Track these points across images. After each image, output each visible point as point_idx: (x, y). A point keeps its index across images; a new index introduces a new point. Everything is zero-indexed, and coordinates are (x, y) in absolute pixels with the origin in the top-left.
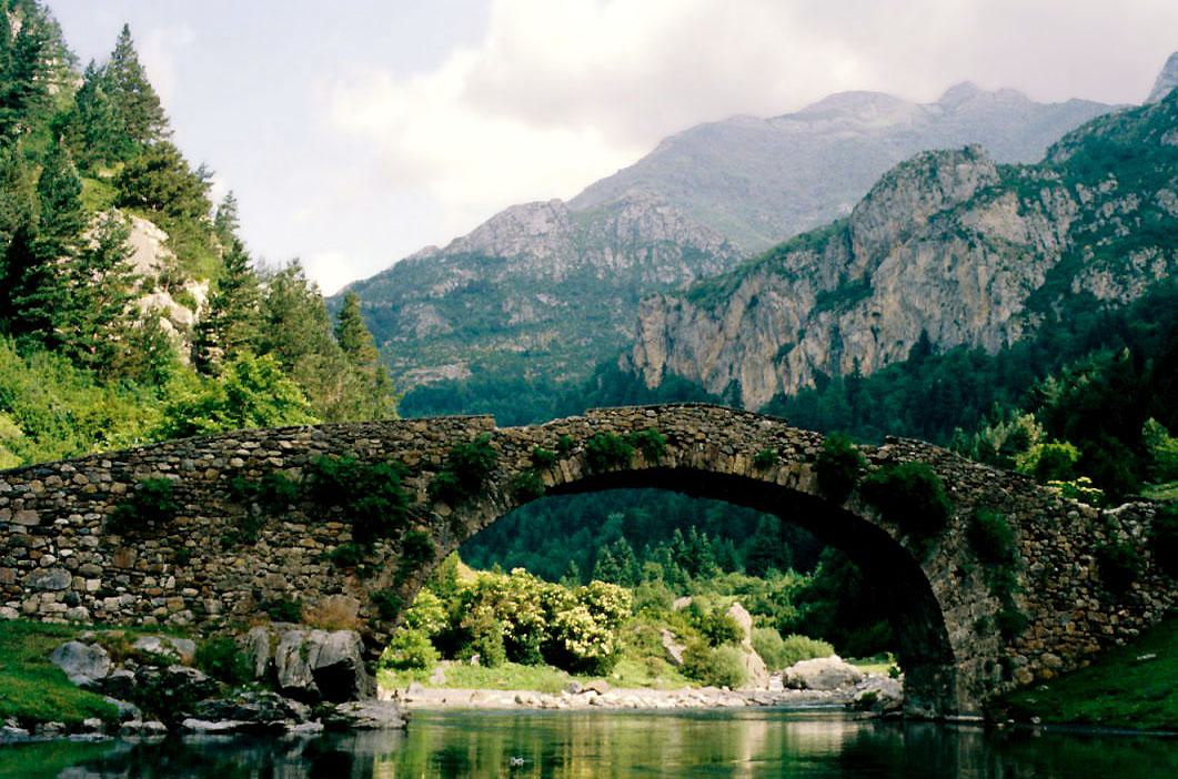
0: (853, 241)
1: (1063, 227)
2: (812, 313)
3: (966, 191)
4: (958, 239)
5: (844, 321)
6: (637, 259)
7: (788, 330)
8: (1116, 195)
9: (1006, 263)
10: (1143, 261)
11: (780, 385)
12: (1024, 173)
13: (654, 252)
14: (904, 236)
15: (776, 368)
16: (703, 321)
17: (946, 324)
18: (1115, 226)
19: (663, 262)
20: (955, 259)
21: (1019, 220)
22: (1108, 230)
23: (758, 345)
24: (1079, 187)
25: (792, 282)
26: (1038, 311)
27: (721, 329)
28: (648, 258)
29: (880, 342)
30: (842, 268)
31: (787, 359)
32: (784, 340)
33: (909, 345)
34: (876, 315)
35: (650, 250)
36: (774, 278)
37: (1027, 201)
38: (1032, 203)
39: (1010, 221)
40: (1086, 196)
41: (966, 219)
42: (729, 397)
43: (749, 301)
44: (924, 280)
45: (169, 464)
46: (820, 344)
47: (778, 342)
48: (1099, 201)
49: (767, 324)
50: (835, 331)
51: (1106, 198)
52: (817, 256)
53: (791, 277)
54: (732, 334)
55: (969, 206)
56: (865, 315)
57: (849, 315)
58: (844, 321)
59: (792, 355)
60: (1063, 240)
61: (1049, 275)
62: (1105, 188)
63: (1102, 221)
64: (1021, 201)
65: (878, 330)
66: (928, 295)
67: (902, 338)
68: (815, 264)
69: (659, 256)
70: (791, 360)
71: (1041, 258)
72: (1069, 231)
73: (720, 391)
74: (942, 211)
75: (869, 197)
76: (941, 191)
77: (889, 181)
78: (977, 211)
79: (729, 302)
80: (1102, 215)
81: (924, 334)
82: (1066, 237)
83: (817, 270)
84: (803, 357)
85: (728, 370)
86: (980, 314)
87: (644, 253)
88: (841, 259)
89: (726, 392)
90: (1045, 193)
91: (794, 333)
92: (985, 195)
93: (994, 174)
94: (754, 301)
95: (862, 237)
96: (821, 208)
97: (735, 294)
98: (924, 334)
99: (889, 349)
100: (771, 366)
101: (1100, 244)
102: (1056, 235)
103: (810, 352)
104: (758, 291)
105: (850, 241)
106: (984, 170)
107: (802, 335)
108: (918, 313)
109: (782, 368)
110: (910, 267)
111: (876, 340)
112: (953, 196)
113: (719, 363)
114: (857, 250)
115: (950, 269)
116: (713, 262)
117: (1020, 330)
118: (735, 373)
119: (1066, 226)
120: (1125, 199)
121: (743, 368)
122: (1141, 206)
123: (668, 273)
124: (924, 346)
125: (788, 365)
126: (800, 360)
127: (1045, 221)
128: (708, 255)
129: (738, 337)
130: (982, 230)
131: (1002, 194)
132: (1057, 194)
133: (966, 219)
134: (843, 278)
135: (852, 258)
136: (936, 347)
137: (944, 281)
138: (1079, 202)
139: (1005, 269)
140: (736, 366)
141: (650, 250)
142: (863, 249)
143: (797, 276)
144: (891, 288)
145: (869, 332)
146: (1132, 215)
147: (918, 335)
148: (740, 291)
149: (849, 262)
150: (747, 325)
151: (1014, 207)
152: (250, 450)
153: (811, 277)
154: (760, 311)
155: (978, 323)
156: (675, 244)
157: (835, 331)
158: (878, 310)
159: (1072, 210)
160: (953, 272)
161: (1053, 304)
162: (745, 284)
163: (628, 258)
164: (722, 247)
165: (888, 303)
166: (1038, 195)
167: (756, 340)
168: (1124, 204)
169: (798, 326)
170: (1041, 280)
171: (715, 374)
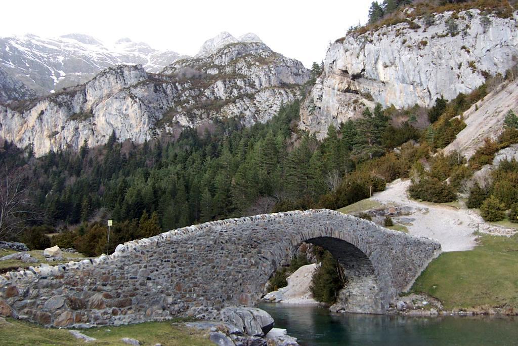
0: (87, 94)
2: (68, 120)
3: (134, 81)
5: (81, 126)
11: (52, 147)
14: (109, 96)
15: (50, 140)
16: (17, 117)
18: (189, 100)
20: (128, 106)
23: (42, 131)
24: (177, 84)
29: (95, 134)
30: (81, 104)
31: (55, 137)
33: (107, 138)
34: (94, 124)
37: (158, 87)
40: (179, 88)
41: (134, 91)
42: (28, 150)
43: (40, 112)
44: (115, 113)
46: (70, 133)
49: (48, 122)
51: (187, 89)
53: (60, 105)
54: (31, 125)
55: (135, 87)
56: (90, 124)
57: (84, 122)
58: (81, 126)
59: (57, 136)
63: (185, 97)
64: (155, 87)
66: (116, 119)
67: (105, 134)
70: (57, 138)
73: (24, 147)
77: (104, 73)
79: (30, 112)
80: (185, 95)
81: (114, 133)
84: (63, 138)
85: (28, 139)
86: (137, 128)
89: (27, 147)
90: (164, 85)
93: (146, 76)
94: (42, 113)
97: (33, 109)
98: (114, 133)
99: (99, 138)
101: (184, 105)
104: (44, 109)
105: (86, 95)
107: (63, 128)
108: (112, 125)
109: (53, 141)
110: (110, 108)
111: (94, 134)
112: (129, 83)
114: (88, 98)
115: (126, 110)
116: (17, 93)
122: (199, 94)
124: (114, 138)
127: (164, 95)
128: (15, 90)
129: (33, 126)
131: (149, 84)
132: (169, 86)
133: (134, 91)
134: (81, 108)
135: (85, 101)
136: (118, 139)
137: (123, 114)
140: (31, 138)
142: (91, 98)
143: (62, 105)
144: (101, 115)
145: (91, 130)
147: (111, 134)
148: (36, 108)
149: (85, 102)
151: (152, 89)
153: (68, 107)
154: (45, 117)
157: (77, 129)
158: (96, 122)
160: (127, 111)
161: (166, 126)
162: (38, 105)
165: (100, 120)
166: (162, 85)
171: (21, 140)
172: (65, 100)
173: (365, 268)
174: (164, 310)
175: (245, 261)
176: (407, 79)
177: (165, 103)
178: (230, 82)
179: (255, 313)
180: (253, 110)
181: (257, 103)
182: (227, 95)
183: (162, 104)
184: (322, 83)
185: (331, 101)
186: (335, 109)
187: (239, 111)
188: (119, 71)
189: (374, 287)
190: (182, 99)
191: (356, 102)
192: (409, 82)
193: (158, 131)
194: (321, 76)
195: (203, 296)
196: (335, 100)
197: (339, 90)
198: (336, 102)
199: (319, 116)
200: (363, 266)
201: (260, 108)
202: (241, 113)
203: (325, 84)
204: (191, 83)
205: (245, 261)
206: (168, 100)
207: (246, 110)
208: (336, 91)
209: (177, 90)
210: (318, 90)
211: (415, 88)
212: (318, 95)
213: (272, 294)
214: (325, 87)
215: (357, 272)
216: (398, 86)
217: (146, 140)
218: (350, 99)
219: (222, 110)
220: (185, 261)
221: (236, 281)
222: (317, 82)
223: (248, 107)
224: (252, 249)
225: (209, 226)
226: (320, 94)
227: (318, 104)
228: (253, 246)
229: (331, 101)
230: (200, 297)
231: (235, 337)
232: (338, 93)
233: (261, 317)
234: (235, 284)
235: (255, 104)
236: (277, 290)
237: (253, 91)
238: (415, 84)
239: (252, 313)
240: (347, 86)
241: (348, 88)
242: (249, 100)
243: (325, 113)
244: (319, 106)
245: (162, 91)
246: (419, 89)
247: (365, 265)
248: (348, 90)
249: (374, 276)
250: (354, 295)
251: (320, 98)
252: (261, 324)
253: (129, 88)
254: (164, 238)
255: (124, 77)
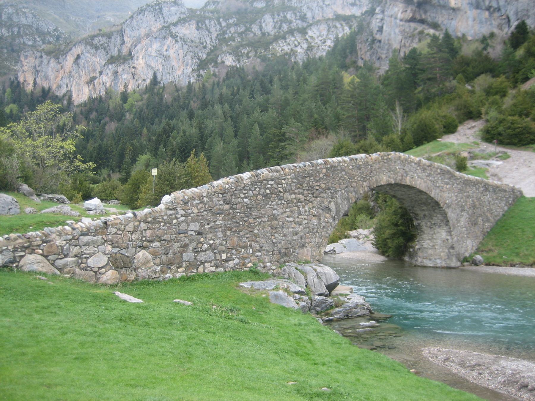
0: (124, 35)
1: (214, 35)
2: (105, 64)
3: (174, 19)
4: (170, 38)
6: (13, 32)
7: (94, 70)
8: (236, 25)
9: (191, 49)
10: (246, 52)
12: (198, 13)
13: (22, 29)
14: (147, 36)
15: (89, 87)
17: (164, 73)
18: (234, 38)
19: (27, 35)
20: (168, 46)
21: (196, 32)
22: (232, 39)
23: (80, 77)
24: (221, 20)
25: (96, 50)
26: (203, 69)
27: (62, 68)
28: (19, 32)
30: (119, 46)
32: (92, 75)
33: (148, 82)
34: (134, 67)
35: (19, 28)
36: (88, 47)
37: (200, 24)
38: (202, 25)
39: (193, 32)
40: (224, 24)
41: (174, 29)
42: (67, 98)
43: (76, 57)
44: (155, 55)
45: (244, 194)
46: (109, 77)
47: (90, 75)
48: (229, 26)
49: (85, 67)
50: (116, 73)
52: (108, 40)
53: (96, 48)
54: (67, 70)
55: (175, 25)
56: (130, 67)
57: (122, 66)
58: (120, 70)
59: (96, 82)
60: (214, 41)
61: (208, 54)
62: (231, 21)
63: (230, 35)
65: (135, 74)
66: (157, 61)
67: (145, 78)
68: (107, 43)
69: (24, 32)
70: (96, 83)
71: (205, 47)
72: (216, 38)
73: (62, 94)
74: (164, 26)
75: (132, 17)
76: (164, 18)
77: (141, 11)
78: (179, 27)
79: (66, 57)
80: (230, 32)
82: (215, 40)
83: (108, 46)
84: (101, 83)
85: (65, 86)
86: (179, 69)
87: (16, 30)
88: (119, 41)
89: (65, 95)
90: (207, 22)
91: (97, 72)
92: (182, 21)
94: (78, 57)
95: (129, 34)
96: (98, 17)
99: (140, 82)
100: (86, 86)
102: (211, 39)
103: (104, 80)
104: (80, 53)
105: (123, 35)
106: (183, 10)
107: (101, 73)
108: (152, 68)
109: (91, 87)
110: (149, 49)
111: (134, 78)
112: (169, 20)
113: (61, 83)
114: (126, 39)
115: (166, 50)
116: (51, 36)
117: (196, 76)
118: (69, 88)
119: (215, 35)
120: (239, 26)
121: (73, 86)
122: (246, 30)
123: (29, 40)
124: (155, 81)
125: (94, 86)
126: (100, 84)
127: (207, 33)
128: (49, 33)
129: (70, 72)
130: (181, 35)
131: (190, 21)
132: (212, 22)
133: (174, 29)
134: (119, 51)
135: (123, 42)
138: (221, 26)
139: (190, 52)
140: (69, 85)
141: (19, 28)
144: (141, 57)
145: (130, 74)
146: (242, 33)
148: (71, 52)
149: (122, 44)
150: (75, 67)
152: (271, 185)
153: (105, 49)
154: (81, 62)
155: (178, 73)
156: (32, 27)
157: (116, 73)
158: (135, 65)
159: (218, 29)
161: (210, 66)
162: (74, 49)
163: (8, 31)
164: (55, 30)
165: (140, 63)
166: (205, 22)
167: (79, 74)
168: (239, 28)
169: (99, 69)
170: (205, 56)
172: (101, 43)
173: (437, 218)
174: (217, 267)
175: (306, 212)
176: (482, 4)
177: (208, 42)
178: (278, 15)
179: (319, 269)
180: (305, 46)
181: (309, 39)
182: (276, 30)
183: (205, 44)
184: (383, 12)
185: (392, 33)
186: (397, 42)
187: (290, 47)
188: (157, 7)
189: (447, 240)
190: (226, 36)
191: (421, 33)
192: (484, 8)
193: (202, 72)
194: (382, 4)
195: (260, 251)
196: (397, 31)
197: (401, 20)
198: (399, 33)
199: (379, 50)
200: (436, 216)
201: (313, 44)
202: (292, 50)
203: (386, 13)
204: (237, 18)
205: (306, 212)
206: (211, 39)
207: (296, 46)
208: (398, 21)
209: (221, 26)
210: (378, 21)
211: (491, 14)
212: (379, 27)
213: (331, 246)
214: (386, 18)
215: (429, 223)
216: (472, 13)
217: (189, 82)
218: (415, 29)
219: (271, 47)
220: (239, 212)
221: (296, 234)
222: (377, 11)
223: (299, 43)
224: (313, 199)
225: (265, 173)
226: (380, 25)
227: (378, 37)
228: (315, 195)
229: (392, 33)
230: (256, 252)
231: (297, 296)
232: (401, 23)
233: (325, 274)
234: (295, 237)
235: (307, 40)
236: (337, 242)
237: (305, 25)
238: (492, 9)
239: (315, 270)
240: (411, 15)
241: (412, 18)
242: (300, 35)
243: (386, 47)
244: (380, 39)
245: (204, 28)
246: (496, 15)
247: (438, 216)
248: (412, 20)
249: (448, 227)
250: (425, 248)
251: (381, 29)
252: (325, 281)
253: (168, 27)
254: (215, 187)
255: (162, 14)
